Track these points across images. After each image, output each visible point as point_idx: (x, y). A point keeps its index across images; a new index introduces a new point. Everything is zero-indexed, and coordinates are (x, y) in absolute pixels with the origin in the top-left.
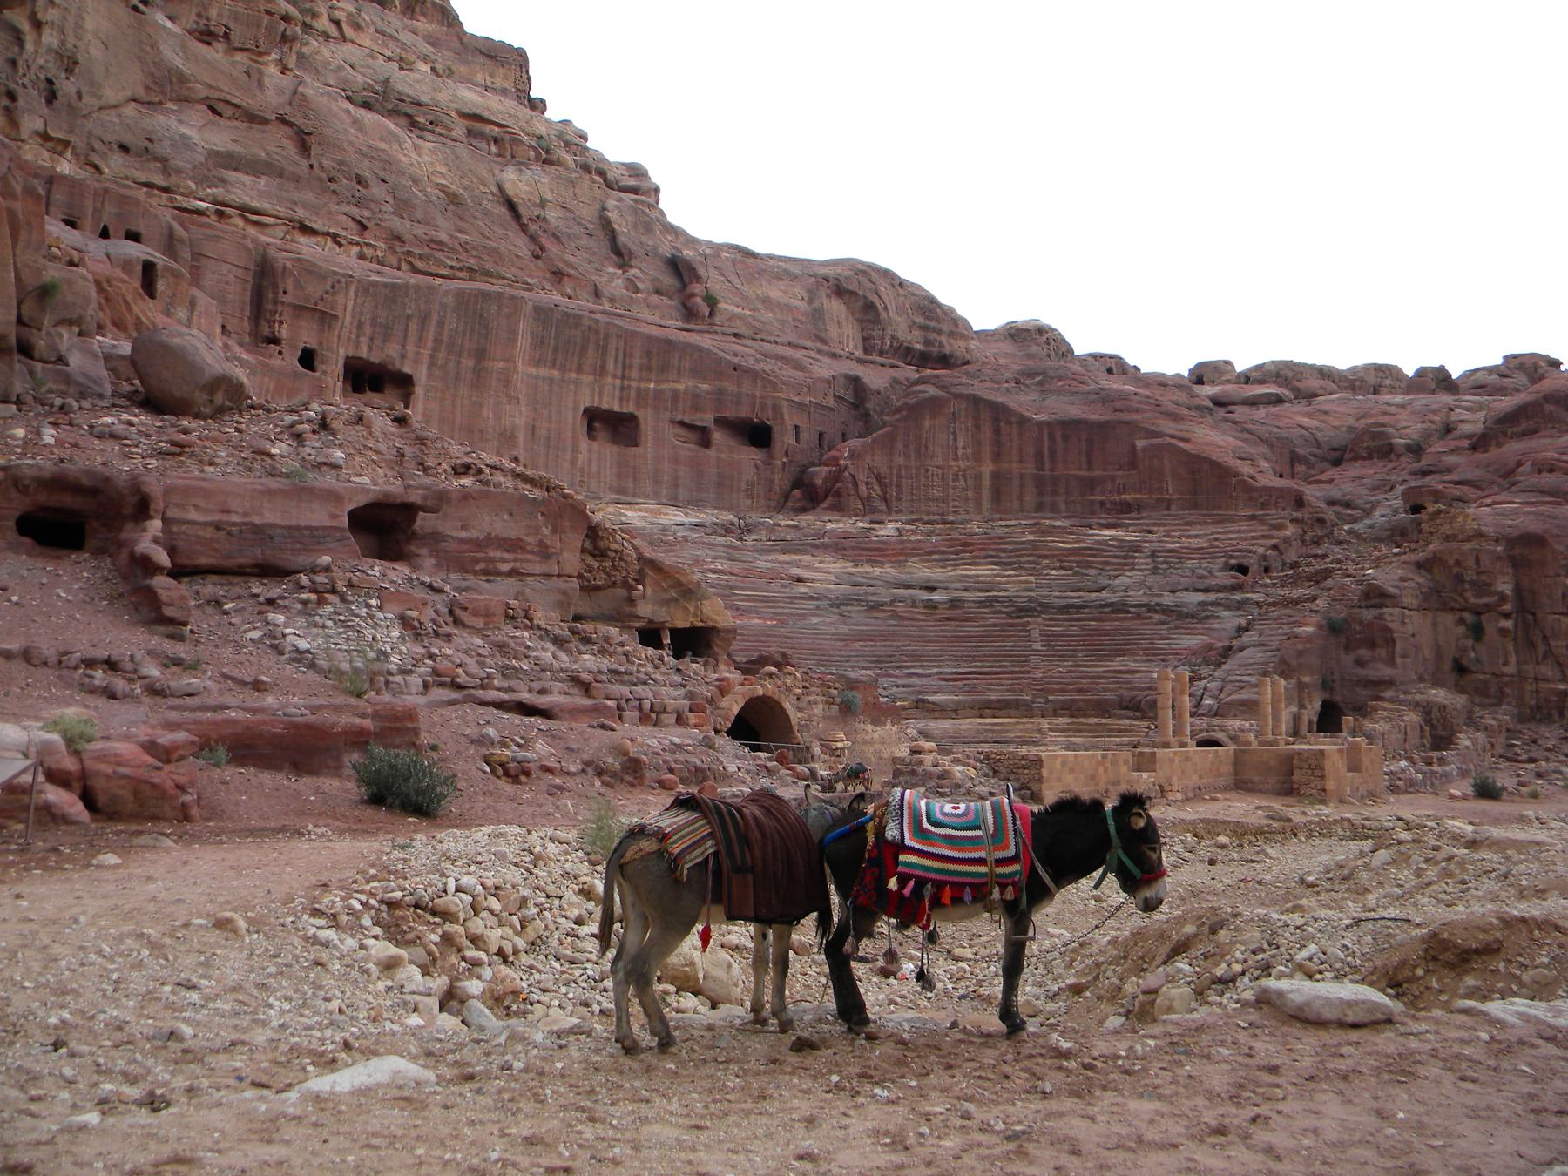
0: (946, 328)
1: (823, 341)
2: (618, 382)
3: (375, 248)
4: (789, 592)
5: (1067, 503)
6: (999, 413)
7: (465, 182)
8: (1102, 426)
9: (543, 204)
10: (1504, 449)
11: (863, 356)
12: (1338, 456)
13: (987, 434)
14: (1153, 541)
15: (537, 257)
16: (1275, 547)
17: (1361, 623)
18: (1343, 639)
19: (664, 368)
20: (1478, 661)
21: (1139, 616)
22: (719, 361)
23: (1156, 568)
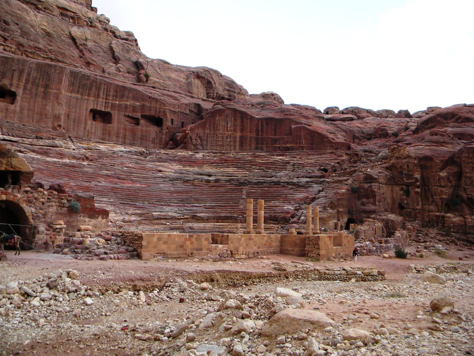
0: (237, 91)
1: (191, 93)
2: (104, 101)
3: (11, 48)
4: (155, 175)
5: (267, 147)
6: (243, 115)
7: (55, 29)
8: (280, 120)
9: (86, 40)
10: (424, 133)
11: (205, 98)
12: (370, 137)
13: (238, 122)
14: (295, 161)
15: (81, 57)
16: (338, 163)
17: (364, 189)
18: (357, 195)
19: (122, 96)
20: (408, 204)
21: (283, 186)
22: (143, 95)
23: (294, 170)
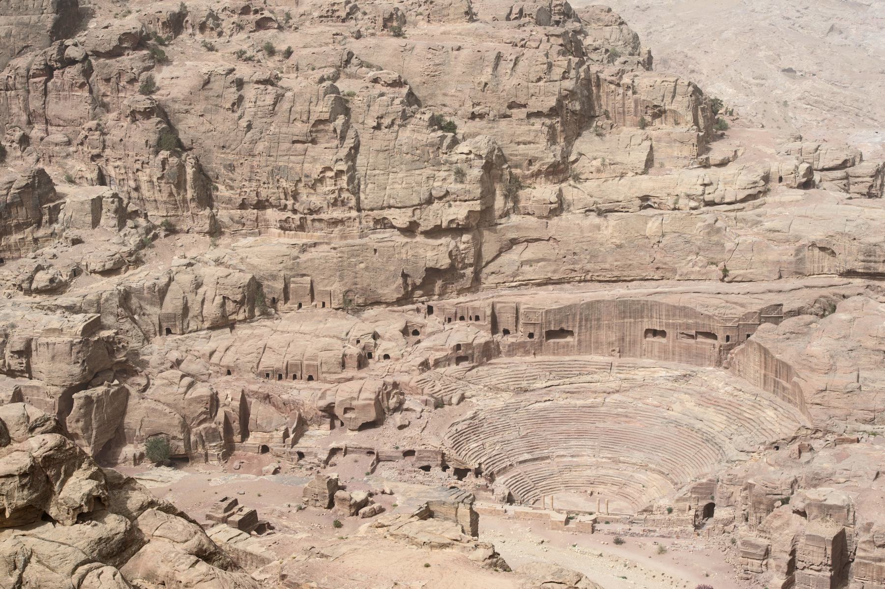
6: (765, 352)
13: (763, 360)
19: (674, 315)
22: (695, 313)
